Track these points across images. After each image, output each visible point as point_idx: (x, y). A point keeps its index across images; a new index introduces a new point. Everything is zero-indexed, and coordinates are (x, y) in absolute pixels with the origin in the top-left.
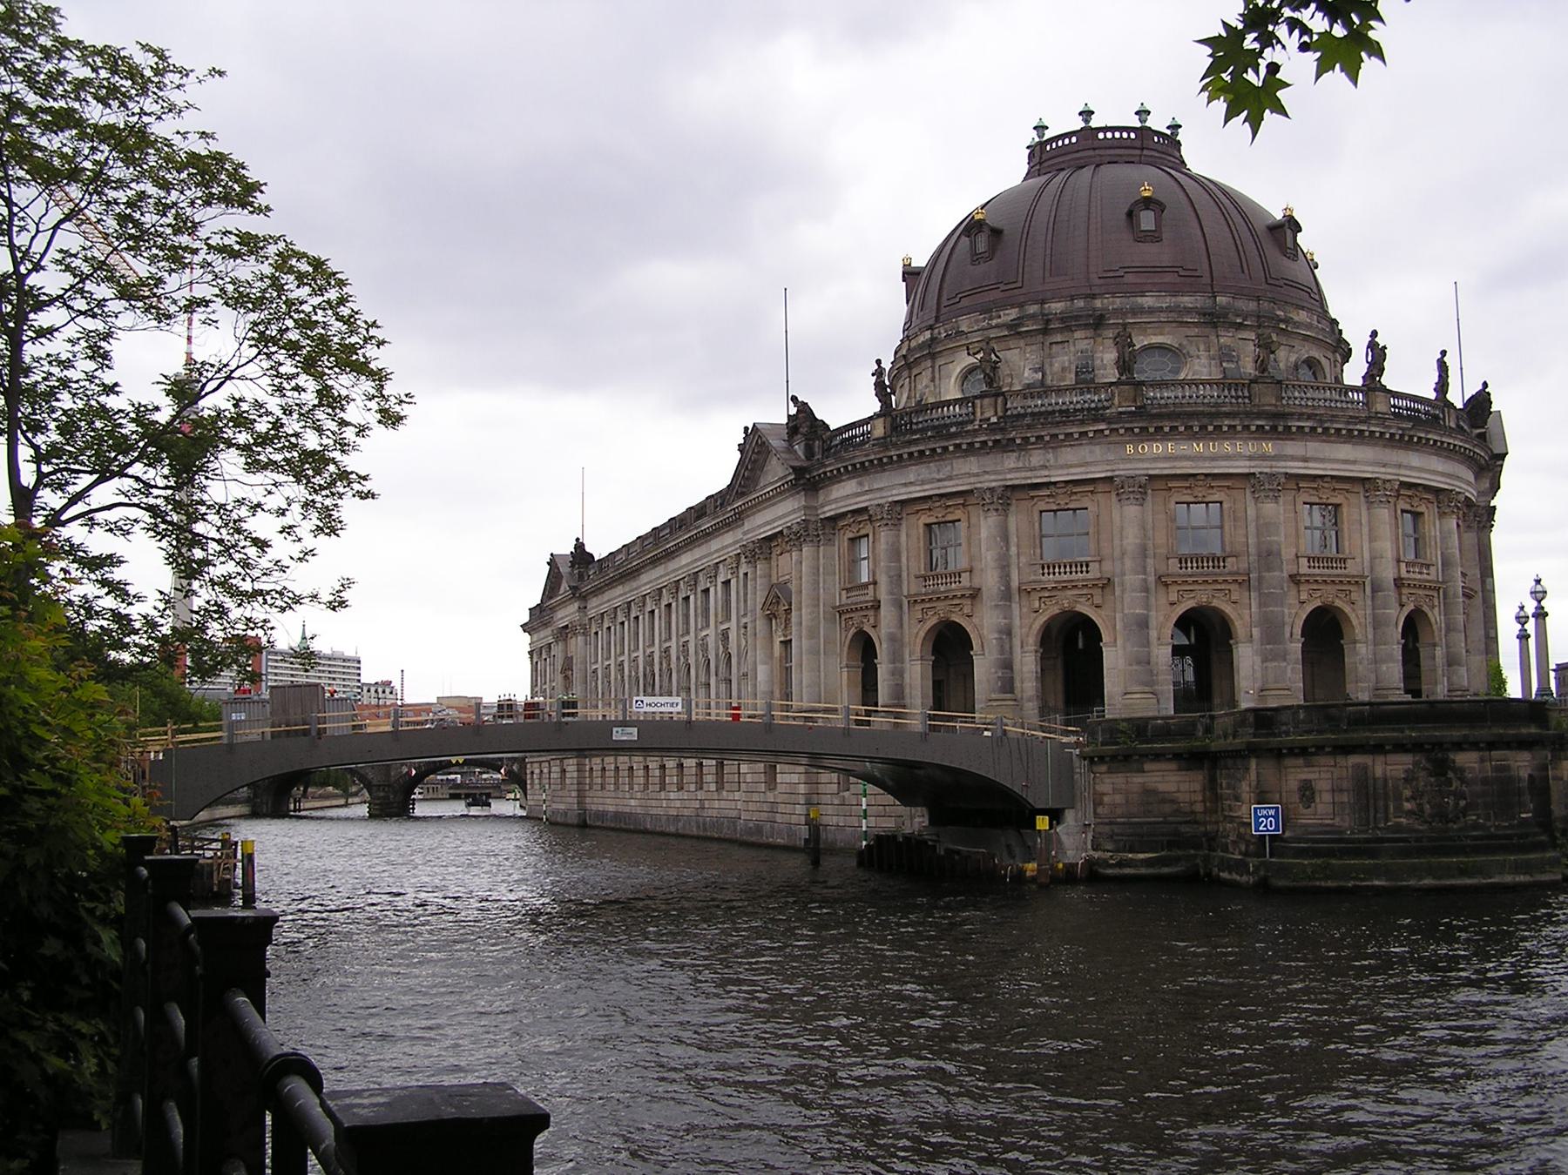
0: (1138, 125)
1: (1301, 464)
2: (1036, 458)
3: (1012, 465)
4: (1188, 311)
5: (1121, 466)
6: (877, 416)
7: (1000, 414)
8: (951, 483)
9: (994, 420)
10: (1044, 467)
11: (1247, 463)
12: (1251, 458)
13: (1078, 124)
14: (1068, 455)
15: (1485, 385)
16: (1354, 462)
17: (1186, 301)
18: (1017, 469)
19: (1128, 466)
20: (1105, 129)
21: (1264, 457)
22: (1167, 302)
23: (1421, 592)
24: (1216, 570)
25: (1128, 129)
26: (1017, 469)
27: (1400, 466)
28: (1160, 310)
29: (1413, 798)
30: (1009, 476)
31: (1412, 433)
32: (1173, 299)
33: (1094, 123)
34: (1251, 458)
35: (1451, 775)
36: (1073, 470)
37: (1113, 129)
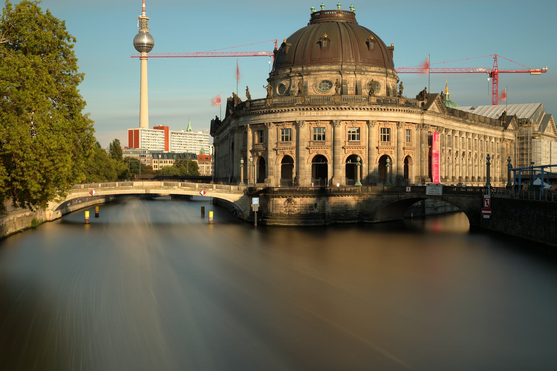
0: (337, 9)
1: (346, 117)
2: (279, 115)
3: (273, 117)
4: (334, 70)
5: (298, 118)
6: (247, 101)
7: (271, 103)
8: (260, 121)
9: (269, 105)
10: (280, 118)
11: (331, 117)
12: (331, 116)
13: (319, 9)
14: (286, 114)
15: (426, 88)
16: (363, 116)
17: (334, 67)
18: (274, 118)
19: (300, 118)
20: (327, 11)
21: (335, 116)
22: (328, 67)
23: (386, 150)
24: (322, 145)
25: (334, 11)
26: (274, 118)
27: (378, 116)
28: (326, 70)
29: (285, 207)
30: (272, 120)
31: (381, 108)
32: (330, 67)
33: (324, 9)
34: (331, 116)
35: (293, 203)
36: (286, 119)
37: (329, 11)
